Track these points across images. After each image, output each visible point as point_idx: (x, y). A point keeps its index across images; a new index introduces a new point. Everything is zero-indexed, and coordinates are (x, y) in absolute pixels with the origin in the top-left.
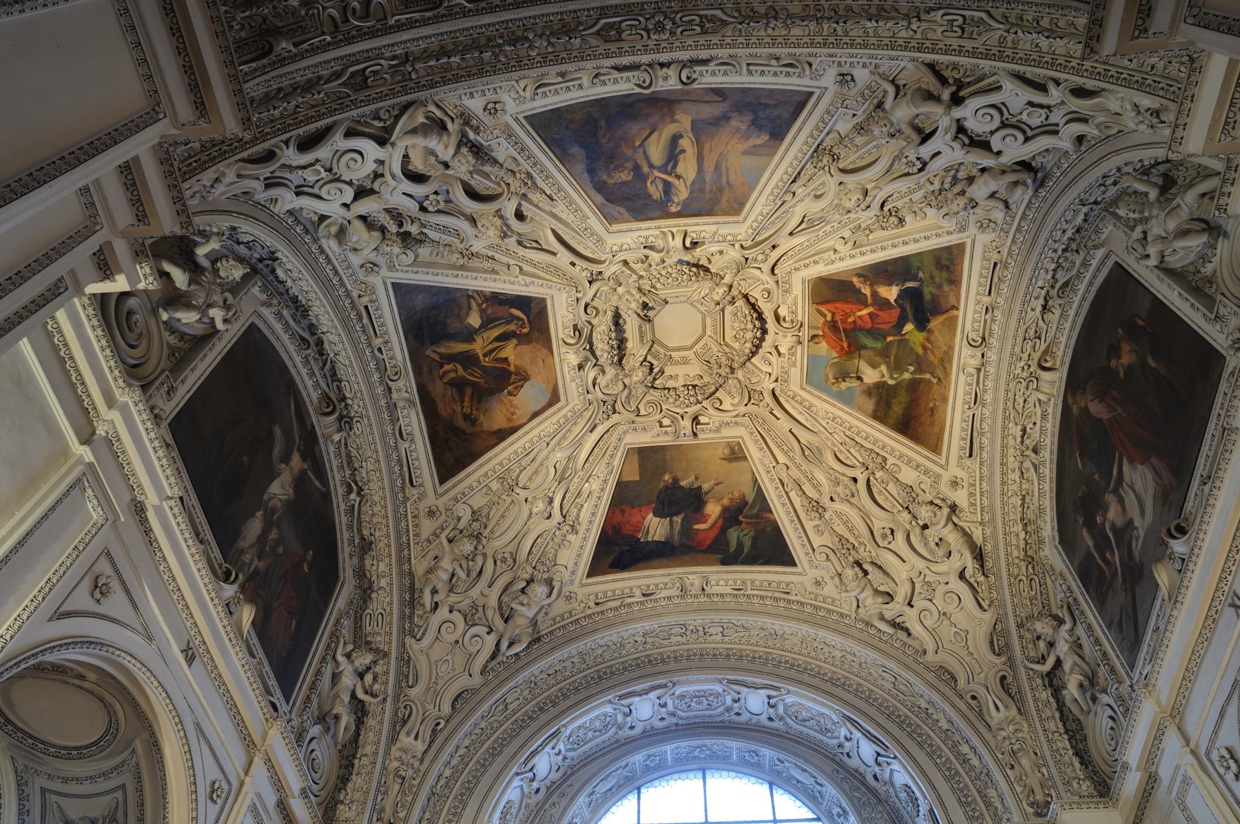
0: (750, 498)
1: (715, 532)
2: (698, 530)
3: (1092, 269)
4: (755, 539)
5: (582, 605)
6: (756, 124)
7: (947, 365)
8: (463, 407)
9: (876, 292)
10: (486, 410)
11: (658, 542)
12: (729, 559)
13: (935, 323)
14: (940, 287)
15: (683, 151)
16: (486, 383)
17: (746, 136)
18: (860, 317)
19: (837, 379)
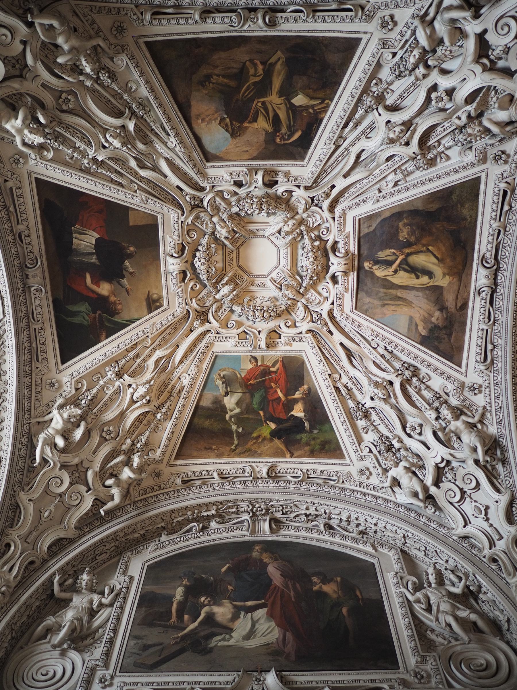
0: (117, 319)
2: (85, 277)
3: (354, 545)
4: (81, 325)
5: (9, 174)
6: (434, 329)
7: (247, 454)
8: (218, 76)
9: (298, 402)
10: (211, 97)
11: (72, 243)
13: (278, 443)
14: (307, 444)
15: (418, 277)
17: (426, 320)
18: (276, 391)
19: (224, 377)
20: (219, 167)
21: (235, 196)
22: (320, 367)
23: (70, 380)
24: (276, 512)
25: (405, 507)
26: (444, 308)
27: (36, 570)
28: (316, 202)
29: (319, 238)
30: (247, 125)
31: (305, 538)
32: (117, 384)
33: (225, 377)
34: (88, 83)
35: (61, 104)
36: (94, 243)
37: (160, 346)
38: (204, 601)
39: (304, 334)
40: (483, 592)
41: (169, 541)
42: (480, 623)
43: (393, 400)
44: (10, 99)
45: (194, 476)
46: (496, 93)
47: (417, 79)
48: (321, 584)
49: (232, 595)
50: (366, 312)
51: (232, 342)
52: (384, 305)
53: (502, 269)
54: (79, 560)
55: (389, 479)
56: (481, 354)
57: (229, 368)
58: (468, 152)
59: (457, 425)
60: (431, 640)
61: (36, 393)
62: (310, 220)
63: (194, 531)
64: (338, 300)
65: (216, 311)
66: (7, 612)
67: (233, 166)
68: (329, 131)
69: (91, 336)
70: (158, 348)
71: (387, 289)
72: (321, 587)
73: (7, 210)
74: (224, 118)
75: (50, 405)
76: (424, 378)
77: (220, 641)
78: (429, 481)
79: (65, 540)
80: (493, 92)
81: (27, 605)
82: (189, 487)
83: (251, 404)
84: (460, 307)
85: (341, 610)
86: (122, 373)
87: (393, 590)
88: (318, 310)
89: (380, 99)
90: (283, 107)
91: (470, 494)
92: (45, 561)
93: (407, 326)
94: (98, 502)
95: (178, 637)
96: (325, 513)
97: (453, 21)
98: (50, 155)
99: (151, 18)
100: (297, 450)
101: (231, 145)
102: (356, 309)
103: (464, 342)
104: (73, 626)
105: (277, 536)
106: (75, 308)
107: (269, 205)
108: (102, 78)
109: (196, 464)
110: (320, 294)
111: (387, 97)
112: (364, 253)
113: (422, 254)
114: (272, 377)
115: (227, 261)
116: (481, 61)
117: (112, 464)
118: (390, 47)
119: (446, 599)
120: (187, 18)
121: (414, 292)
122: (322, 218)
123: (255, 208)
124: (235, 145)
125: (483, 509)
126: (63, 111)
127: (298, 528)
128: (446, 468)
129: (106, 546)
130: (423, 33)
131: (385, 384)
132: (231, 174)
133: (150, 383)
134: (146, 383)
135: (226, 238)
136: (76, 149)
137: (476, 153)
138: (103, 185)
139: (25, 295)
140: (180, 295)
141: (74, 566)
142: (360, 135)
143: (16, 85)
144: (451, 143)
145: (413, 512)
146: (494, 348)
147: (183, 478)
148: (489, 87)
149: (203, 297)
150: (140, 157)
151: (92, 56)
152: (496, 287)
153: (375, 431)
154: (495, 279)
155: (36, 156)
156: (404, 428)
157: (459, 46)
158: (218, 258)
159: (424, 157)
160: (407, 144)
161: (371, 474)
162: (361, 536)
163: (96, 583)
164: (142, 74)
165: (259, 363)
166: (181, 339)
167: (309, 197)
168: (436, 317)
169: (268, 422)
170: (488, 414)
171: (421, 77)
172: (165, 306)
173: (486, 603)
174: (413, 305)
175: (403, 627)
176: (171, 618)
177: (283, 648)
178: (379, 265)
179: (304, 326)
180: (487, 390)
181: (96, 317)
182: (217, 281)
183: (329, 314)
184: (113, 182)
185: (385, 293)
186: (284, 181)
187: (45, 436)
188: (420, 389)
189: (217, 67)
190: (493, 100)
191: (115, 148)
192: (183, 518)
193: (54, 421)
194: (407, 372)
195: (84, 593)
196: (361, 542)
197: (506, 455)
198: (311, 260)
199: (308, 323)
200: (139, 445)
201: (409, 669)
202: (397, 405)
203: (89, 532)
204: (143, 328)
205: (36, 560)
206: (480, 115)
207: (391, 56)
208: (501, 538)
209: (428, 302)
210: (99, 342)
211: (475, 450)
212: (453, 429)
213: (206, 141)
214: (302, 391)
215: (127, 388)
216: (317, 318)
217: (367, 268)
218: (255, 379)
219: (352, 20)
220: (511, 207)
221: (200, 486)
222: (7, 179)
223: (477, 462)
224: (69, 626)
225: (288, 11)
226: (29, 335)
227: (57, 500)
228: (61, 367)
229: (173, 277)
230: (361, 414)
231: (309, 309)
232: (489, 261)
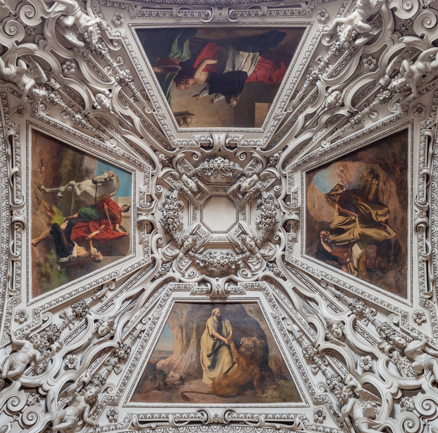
0: (172, 84)
1: (200, 58)
2: (213, 59)
7: (35, 200)
8: (378, 185)
9: (87, 250)
10: (361, 178)
13: (47, 231)
14: (46, 260)
15: (209, 356)
16: (357, 200)
17: (170, 366)
18: (97, 229)
19: (111, 180)
20: (302, 183)
21: (275, 195)
22: (121, 271)
23: (122, 35)
26: (182, 381)
28: (271, 265)
29: (238, 268)
30: (337, 207)
32: (113, 80)
33: (111, 182)
34: (382, 81)
35: (368, 58)
36: (243, 70)
37: (143, 121)
39: (151, 256)
43: (96, 341)
45: (16, 148)
46: (374, 406)
47: (379, 344)
50: (173, 311)
51: (144, 188)
52: (181, 328)
53: (223, 428)
56: (145, 418)
57: (119, 185)
58: (323, 390)
62: (254, 260)
64: (184, 286)
65: (171, 175)
67: (302, 195)
68: (332, 275)
69: (159, 59)
70: (142, 119)
71: (196, 330)
74: (343, 189)
75: (100, 15)
76: (118, 368)
78: (26, 379)
80: (374, 404)
82: (5, 142)
83: (85, 205)
84: (185, 396)
86: (123, 84)
88: (174, 268)
89: (361, 315)
90: (351, 237)
91: (17, 420)
99: (426, 135)
100: (40, 250)
101: (320, 193)
102: (176, 302)
103: (154, 402)
107: (270, 224)
108: (385, 92)
109: (27, 150)
110: (186, 270)
111: (362, 321)
112: (227, 307)
113: (230, 358)
114: (110, 225)
115: (216, 186)
116: (399, 391)
118: (403, 321)
120: (424, 163)
121: (195, 354)
122: (257, 270)
123: (268, 212)
124: (320, 196)
126: (361, 58)
128: (38, 395)
130: (419, 345)
131: (111, 331)
132: (296, 193)
133: (112, 110)
134: (112, 107)
135: (240, 187)
136: (327, 65)
137: (323, 396)
138: (295, 84)
139: (204, 4)
140: (190, 143)
142: (330, 300)
143: (390, 25)
144: (329, 375)
146: (153, 429)
147: (15, 136)
149: (185, 164)
150: (315, 117)
151: (405, 88)
152: (206, 425)
153: (65, 325)
154: (214, 423)
155: (326, 31)
156: (70, 353)
157: (408, 374)
158: (219, 178)
159: (315, 354)
161: (21, 323)
164: (384, 125)
166: (148, 141)
167: (276, 258)
168: (173, 375)
169: (67, 221)
171: (381, 347)
174: (183, 354)
178: (217, 322)
179: (158, 255)
180: (114, 427)
181: (175, 65)
182: (200, 176)
183: (169, 278)
184: (295, 92)
185: (192, 328)
186: (289, 237)
187: (76, 8)
188: (106, 365)
189: (385, 184)
190: (369, 405)
191: (326, 97)
193: (88, 18)
194: (122, 352)
198: (222, 261)
199: (162, 259)
200: (52, 95)
204: (162, 107)
207: (396, 322)
209: (187, 367)
210: (152, 66)
211: (62, 420)
214: (97, 254)
215: (109, 88)
216: (166, 267)
217: (213, 311)
218: (108, 210)
219: (421, 291)
220: (279, 430)
222: (308, 4)
223: (50, 424)
225: (427, 242)
227: (12, 12)
228: (133, 29)
229: (206, 137)
230: (80, 311)
231: (173, 260)
232: (230, 417)
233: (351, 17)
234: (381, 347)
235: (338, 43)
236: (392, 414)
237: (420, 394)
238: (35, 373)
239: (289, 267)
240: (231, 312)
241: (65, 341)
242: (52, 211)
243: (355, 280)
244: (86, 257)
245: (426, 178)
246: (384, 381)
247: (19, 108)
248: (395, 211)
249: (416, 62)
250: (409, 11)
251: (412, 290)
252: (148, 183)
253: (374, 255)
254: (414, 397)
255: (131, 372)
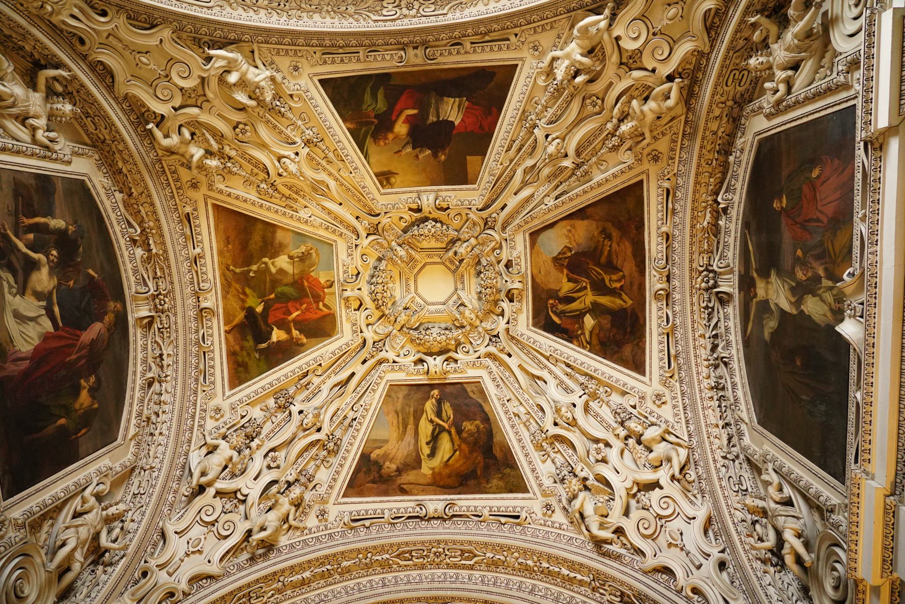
0: (369, 140)
1: (398, 107)
2: (414, 108)
3: (134, 414)
6: (377, 465)
7: (225, 282)
8: (610, 246)
10: (591, 239)
11: (449, 96)
12: (383, 79)
13: (240, 316)
14: (242, 348)
15: (428, 443)
16: (588, 264)
17: (386, 456)
18: (298, 310)
24: (161, 321)
25: (185, 463)
27: (72, 46)
28: (494, 339)
29: (458, 344)
30: (565, 273)
31: (135, 358)
34: (610, 126)
36: (449, 119)
38: (52, 255)
40: (106, 569)
41: (116, 202)
42: (69, 577)
43: (301, 434)
44: (599, 50)
45: (195, 226)
48: (88, 387)
49: (63, 287)
50: (388, 395)
52: (397, 413)
54: (86, 98)
55: (215, 442)
58: (552, 480)
59: (285, 504)
60: (41, 526)
61: (287, 50)
63: (130, 230)
66: (16, 10)
72: (85, 388)
73: (486, 33)
74: (571, 251)
77: (8, 282)
78: (220, 485)
79: (111, 80)
81: (26, 35)
82: (181, 221)
84: (402, 488)
85: (63, 417)
87: (92, 469)
88: (387, 347)
89: (594, 396)
90: (583, 306)
92: (84, 57)
93: (378, 438)
94: (159, 119)
95: (5, 230)
96: (166, 376)
97: (669, 460)
98: (541, 82)
100: (235, 339)
102: (391, 385)
104: (5, 98)
105: (134, 326)
106: (380, 95)
108: (613, 139)
110: (402, 347)
116: (635, 485)
117: (207, 135)
119: (92, 531)
120: (663, 219)
121: (413, 441)
125: (199, 548)
126: (584, 99)
127: (145, 348)
129: (106, 129)
134: (301, 172)
136: (546, 108)
139: (395, 44)
141: (78, 92)
143: (615, 58)
144: (558, 464)
145: (181, 473)
148: (613, 494)
151: (636, 133)
152: (426, 521)
154: (434, 518)
156: (273, 450)
160: (556, 424)
161: (217, 420)
162: (145, 419)
163: (60, 122)
164: (615, 176)
165: (326, 290)
170: (298, 533)
171: (616, 433)
172: (383, 191)
173: (94, 576)
175: (53, 493)
176: (27, 218)
177: (11, 359)
179: (369, 335)
185: (409, 413)
187: (240, 61)
189: (619, 246)
192: (144, 216)
193: (257, 71)
194: (332, 444)
195: (46, 106)
196: (139, 421)
197: (261, 560)
198: (439, 339)
200: (229, 165)
201: (6, 513)
202: (296, 439)
203: (122, 109)
205: (86, 47)
206: (586, 488)
207: (633, 404)
208: (170, 575)
211: (263, 529)
212: (280, 501)
213: (549, 233)
214: (299, 337)
217: (432, 393)
219: (661, 368)
220: (504, 524)
221: (183, 234)
222: (518, 36)
223: (249, 533)
224: (6, 93)
226: (352, 46)
228: (316, 79)
232: (451, 511)
233: (568, 49)
234: (616, 433)
235: (555, 82)
236: (627, 513)
237: (657, 489)
238: (234, 476)
239: (514, 341)
240: (451, 394)
241: (267, 436)
242: (244, 293)
243: (587, 356)
244: (287, 341)
245: (665, 236)
246: (618, 473)
247: (193, 181)
248: (630, 275)
249: (648, 102)
250: (635, 39)
251: (651, 367)
252: (352, 255)
253: (609, 326)
254: (650, 492)
255: (341, 466)
